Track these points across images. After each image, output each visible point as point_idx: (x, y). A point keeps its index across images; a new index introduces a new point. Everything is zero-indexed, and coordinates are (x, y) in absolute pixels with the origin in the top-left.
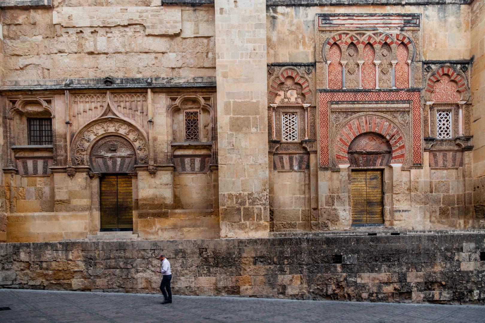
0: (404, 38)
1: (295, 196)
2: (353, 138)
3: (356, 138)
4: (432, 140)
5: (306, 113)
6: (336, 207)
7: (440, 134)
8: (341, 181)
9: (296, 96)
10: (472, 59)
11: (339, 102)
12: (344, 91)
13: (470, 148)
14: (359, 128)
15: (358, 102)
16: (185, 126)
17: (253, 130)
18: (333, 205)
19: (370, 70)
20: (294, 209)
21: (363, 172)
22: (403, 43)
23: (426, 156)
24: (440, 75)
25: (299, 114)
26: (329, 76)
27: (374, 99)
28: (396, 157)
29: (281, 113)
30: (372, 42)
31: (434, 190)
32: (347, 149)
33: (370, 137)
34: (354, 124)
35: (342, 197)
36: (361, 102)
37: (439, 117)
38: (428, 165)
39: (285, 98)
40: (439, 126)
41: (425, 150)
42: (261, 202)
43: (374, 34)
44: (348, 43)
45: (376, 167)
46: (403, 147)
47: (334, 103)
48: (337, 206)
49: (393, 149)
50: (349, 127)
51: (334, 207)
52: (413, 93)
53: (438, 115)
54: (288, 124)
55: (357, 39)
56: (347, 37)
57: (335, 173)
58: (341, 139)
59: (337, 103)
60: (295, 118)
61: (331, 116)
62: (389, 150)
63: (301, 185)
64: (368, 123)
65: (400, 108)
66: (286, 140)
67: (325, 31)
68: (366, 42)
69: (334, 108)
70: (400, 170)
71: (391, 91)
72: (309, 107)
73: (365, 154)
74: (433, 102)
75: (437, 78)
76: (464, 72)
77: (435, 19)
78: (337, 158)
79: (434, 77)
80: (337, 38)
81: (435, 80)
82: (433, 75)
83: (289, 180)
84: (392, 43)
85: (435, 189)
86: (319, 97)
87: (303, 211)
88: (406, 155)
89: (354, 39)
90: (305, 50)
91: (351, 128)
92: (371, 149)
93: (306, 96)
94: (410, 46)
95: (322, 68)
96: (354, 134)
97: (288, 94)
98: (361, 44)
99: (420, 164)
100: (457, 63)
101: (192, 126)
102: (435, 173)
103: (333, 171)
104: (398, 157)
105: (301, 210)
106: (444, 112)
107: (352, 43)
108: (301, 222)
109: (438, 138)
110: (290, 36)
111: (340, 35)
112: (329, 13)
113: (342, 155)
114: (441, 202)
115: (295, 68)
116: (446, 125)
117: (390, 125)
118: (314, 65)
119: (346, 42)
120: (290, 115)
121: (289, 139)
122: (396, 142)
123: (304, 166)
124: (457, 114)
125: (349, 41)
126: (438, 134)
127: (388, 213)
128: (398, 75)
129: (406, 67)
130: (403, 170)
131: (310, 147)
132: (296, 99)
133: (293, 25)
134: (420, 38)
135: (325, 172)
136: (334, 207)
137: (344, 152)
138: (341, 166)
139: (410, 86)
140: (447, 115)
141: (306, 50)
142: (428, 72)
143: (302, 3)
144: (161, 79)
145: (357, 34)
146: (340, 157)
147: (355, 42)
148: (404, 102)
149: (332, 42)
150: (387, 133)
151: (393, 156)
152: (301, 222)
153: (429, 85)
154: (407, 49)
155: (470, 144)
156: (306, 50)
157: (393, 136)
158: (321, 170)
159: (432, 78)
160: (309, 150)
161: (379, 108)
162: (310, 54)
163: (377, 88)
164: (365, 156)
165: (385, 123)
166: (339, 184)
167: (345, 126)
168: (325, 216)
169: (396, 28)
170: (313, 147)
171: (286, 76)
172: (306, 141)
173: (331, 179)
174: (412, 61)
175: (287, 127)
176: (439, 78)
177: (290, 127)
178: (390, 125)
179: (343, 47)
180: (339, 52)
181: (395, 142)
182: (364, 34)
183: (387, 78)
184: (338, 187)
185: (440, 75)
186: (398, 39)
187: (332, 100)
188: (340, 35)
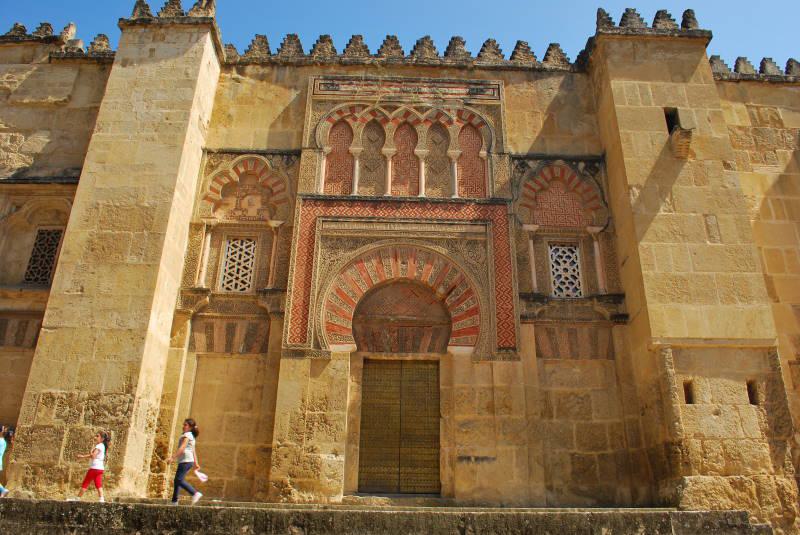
1: (230, 413)
5: (275, 237)
7: (560, 290)
9: (258, 205)
10: (604, 156)
11: (339, 217)
13: (622, 318)
16: (30, 256)
17: (131, 259)
22: (470, 124)
23: (527, 332)
24: (546, 179)
25: (260, 240)
28: (459, 333)
29: (224, 237)
31: (555, 413)
35: (331, 419)
38: (533, 353)
39: (236, 209)
40: (556, 274)
41: (524, 318)
42: (113, 418)
46: (475, 311)
49: (454, 315)
54: (237, 259)
55: (384, 115)
58: (339, 291)
59: (335, 220)
60: (253, 246)
63: (248, 389)
66: (228, 289)
67: (325, 101)
69: (327, 230)
75: (540, 184)
76: (593, 175)
85: (559, 410)
87: (243, 453)
89: (379, 114)
97: (245, 203)
100: (578, 159)
101: (43, 256)
102: (554, 372)
105: (238, 449)
106: (563, 246)
107: (374, 121)
108: (234, 478)
113: (338, 323)
115: (263, 158)
116: (570, 272)
121: (233, 288)
122: (459, 301)
124: (590, 251)
125: (370, 118)
126: (554, 288)
130: (475, 358)
132: (259, 211)
140: (570, 250)
141: (289, 129)
144: (7, 170)
147: (378, 119)
149: (336, 117)
152: (234, 478)
153: (525, 196)
155: (621, 310)
156: (289, 129)
157: (452, 291)
168: (286, 463)
169: (457, 100)
171: (242, 170)
172: (265, 292)
175: (233, 264)
176: (546, 184)
177: (239, 264)
178: (446, 265)
181: (459, 299)
182: (396, 108)
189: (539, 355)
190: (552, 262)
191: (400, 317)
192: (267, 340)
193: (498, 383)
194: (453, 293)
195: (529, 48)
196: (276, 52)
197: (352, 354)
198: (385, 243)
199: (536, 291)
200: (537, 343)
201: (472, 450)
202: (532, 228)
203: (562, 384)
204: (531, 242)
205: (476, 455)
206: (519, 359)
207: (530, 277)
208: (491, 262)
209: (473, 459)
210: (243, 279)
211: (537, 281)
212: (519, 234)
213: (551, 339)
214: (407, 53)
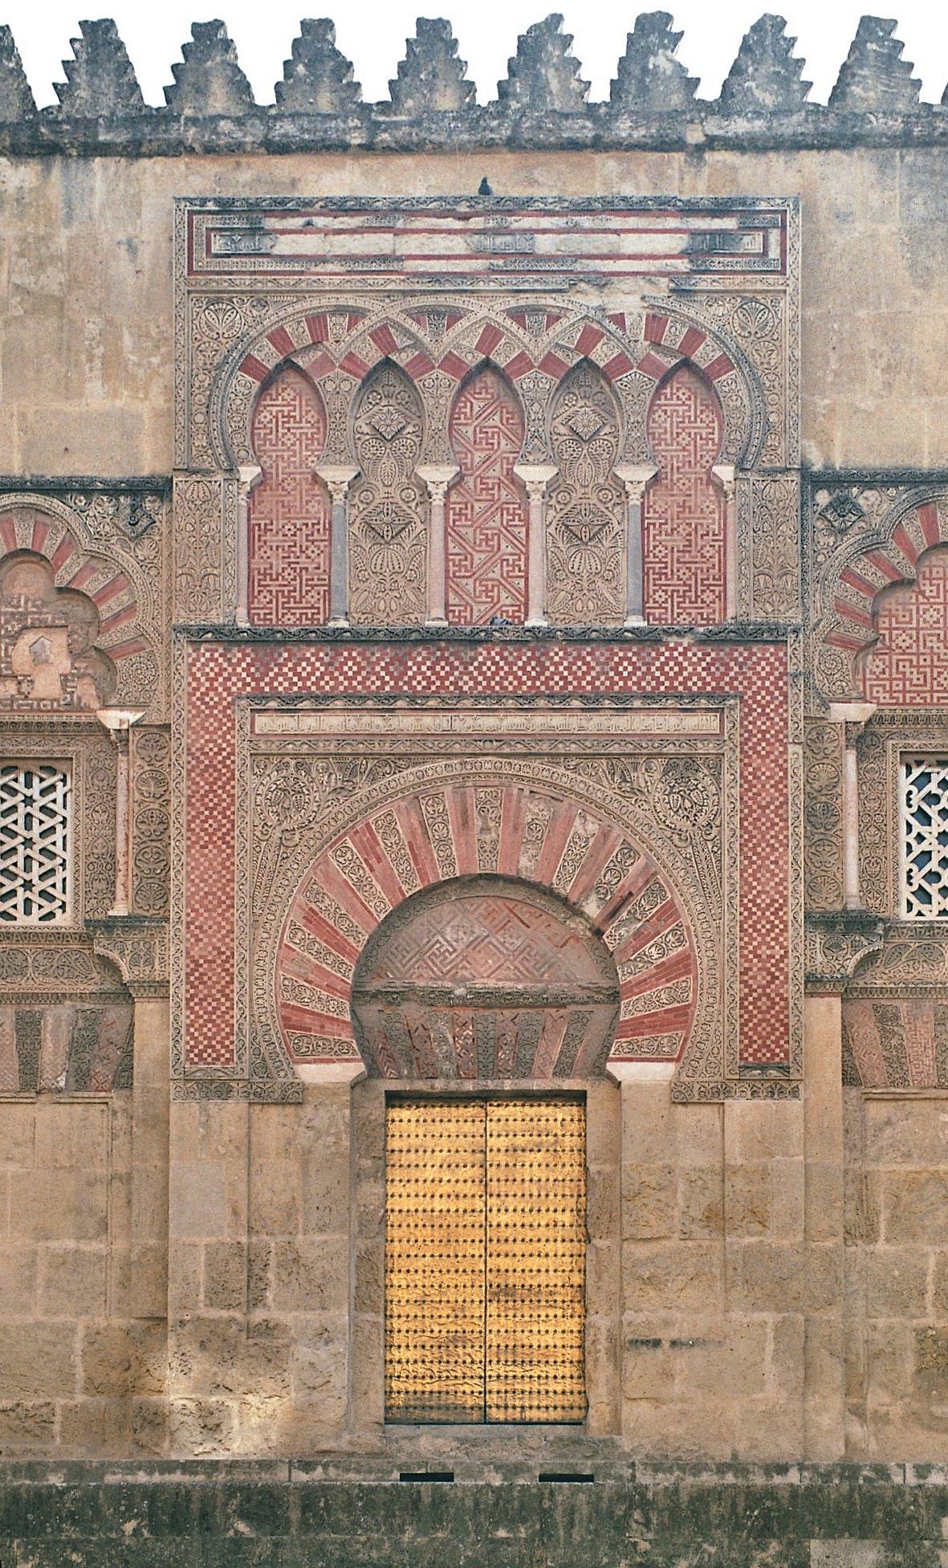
0: (695, 336)
1: (54, 1244)
2: (381, 906)
3: (406, 908)
4: (859, 923)
6: (277, 1315)
8: (305, 1164)
11: (299, 698)
12: (335, 639)
14: (423, 853)
15: (417, 703)
18: (256, 1301)
19: (496, 522)
20: (39, 1325)
21: (471, 1111)
22: (686, 364)
24: (909, 551)
26: (251, 554)
27: (510, 684)
28: (637, 1026)
30: (501, 361)
31: (883, 1228)
32: (347, 975)
34: (390, 827)
36: (432, 703)
37: (916, 799)
41: (814, 984)
43: (517, 315)
44: (362, 366)
45: (536, 1085)
47: (273, 704)
48: (282, 1305)
49: (625, 976)
50: (363, 849)
51: (258, 1315)
52: (740, 653)
53: (905, 784)
55: (417, 343)
56: (354, 333)
57: (274, 1112)
58: (312, 918)
59: (289, 704)
62: (605, 983)
65: (664, 739)
68: (472, 360)
70: (665, 1103)
71: (617, 638)
72: (136, 725)
73: (464, 1003)
74: (871, 708)
77: (884, 230)
78: (287, 1023)
79: (878, 562)
80: (301, 335)
81: (881, 581)
82: (868, 550)
83: (16, 1152)
84: (621, 364)
85: (894, 1219)
86: (183, 669)
87: (93, 1338)
88: (699, 1014)
89: (400, 341)
90: (118, 403)
91: (370, 849)
92: (502, 973)
93: (119, 663)
94: (731, 383)
95: (206, 507)
98: (437, 372)
99: (785, 1069)
102: (888, 1123)
103: (259, 1098)
104: (653, 1027)
105: (81, 1332)
109: (904, 915)
110: (31, 323)
111: (317, 323)
112: (264, 193)
114: (929, 1297)
117: (605, 835)
118: (161, 488)
119: (351, 357)
120: (29, 775)
122: (640, 938)
123: (103, 1071)
125: (371, 355)
127: (603, 1357)
128: (661, 552)
129: (707, 501)
130: (680, 1096)
131: (134, 963)
133: (53, 259)
134: (789, 339)
135: (213, 1105)
136: (258, 1315)
137: (330, 988)
138: (311, 1073)
139: (731, 612)
142: (843, 532)
143: (101, 138)
145: (417, 315)
146: (308, 1019)
147: (402, 359)
148: (686, 701)
149: (268, 356)
150: (585, 879)
151: (623, 1017)
153: (841, 608)
154: (715, 402)
157: (624, 901)
158: (189, 1093)
159: (866, 569)
160: (126, 977)
161: (539, 738)
162: (148, 423)
163: (535, 621)
164: (466, 1014)
165: (578, 822)
166: (295, 1181)
167: (334, 841)
170: (149, 962)
172: (110, 925)
173: (248, 1150)
174: (740, 467)
178: (605, 835)
179: (330, 386)
180: (313, 416)
181: (637, 934)
182: (454, 316)
183: (595, 563)
184: (285, 1198)
185: (909, 551)
186: (656, 344)
187: (258, 688)
188: (317, 323)
189: (850, 1078)
190: (905, 813)
191: (479, 984)
192: (129, 1054)
194: (624, 915)
195: (899, 46)
196: (55, 101)
197: (357, 1084)
198: (436, 768)
199: (854, 904)
200: (847, 1048)
201: (667, 1323)
202: (857, 712)
203: (908, 1156)
204: (851, 757)
205: (674, 1334)
206: (795, 1093)
207: (842, 863)
208: (730, 824)
209: (666, 1345)
210: (45, 885)
211: (862, 872)
212: (817, 727)
213: (886, 1034)
214: (486, 95)
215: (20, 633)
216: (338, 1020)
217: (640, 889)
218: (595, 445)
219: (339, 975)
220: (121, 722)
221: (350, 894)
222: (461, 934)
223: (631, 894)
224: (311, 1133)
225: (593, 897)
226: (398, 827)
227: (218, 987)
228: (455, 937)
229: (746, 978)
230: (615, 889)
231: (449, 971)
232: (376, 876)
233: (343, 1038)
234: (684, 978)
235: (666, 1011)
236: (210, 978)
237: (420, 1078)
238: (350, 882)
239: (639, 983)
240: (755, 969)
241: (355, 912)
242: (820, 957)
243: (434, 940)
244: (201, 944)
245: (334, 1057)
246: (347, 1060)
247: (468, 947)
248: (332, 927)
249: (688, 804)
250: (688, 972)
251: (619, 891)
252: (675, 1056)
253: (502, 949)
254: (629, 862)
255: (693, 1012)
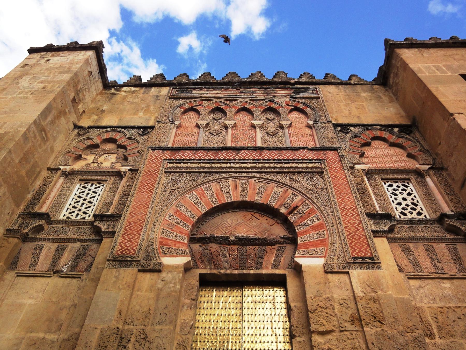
14: (220, 196)
33: (245, 213)
61: (163, 177)
64: (240, 189)
73: (234, 243)
78: (161, 243)
96: (207, 204)
104: (312, 246)
137: (181, 232)
138: (167, 261)
146: (170, 242)
166: (152, 302)
181: (301, 216)
184: (146, 309)
193: (359, 292)
194: (295, 212)
215: (103, 155)
216: (182, 243)
217: (300, 205)
218: (273, 121)
219: (185, 229)
220: (126, 170)
221: (193, 206)
222: (233, 221)
223: (297, 207)
224: (163, 283)
225: (283, 207)
226: (212, 189)
227: (136, 230)
228: (231, 222)
229: (347, 229)
230: (291, 205)
231: (228, 232)
232: (203, 201)
233: (183, 248)
234: (322, 230)
235: (317, 241)
236: (134, 228)
237: (215, 269)
238: (193, 203)
239: (304, 232)
240: (350, 227)
241: (194, 211)
242: (373, 227)
243: (223, 223)
244: (133, 218)
245: (178, 255)
246: (184, 256)
247: (236, 225)
248: (184, 215)
249: (314, 184)
250: (324, 228)
251: (293, 205)
252: (324, 255)
253: (249, 226)
254: (295, 198)
255: (328, 241)
